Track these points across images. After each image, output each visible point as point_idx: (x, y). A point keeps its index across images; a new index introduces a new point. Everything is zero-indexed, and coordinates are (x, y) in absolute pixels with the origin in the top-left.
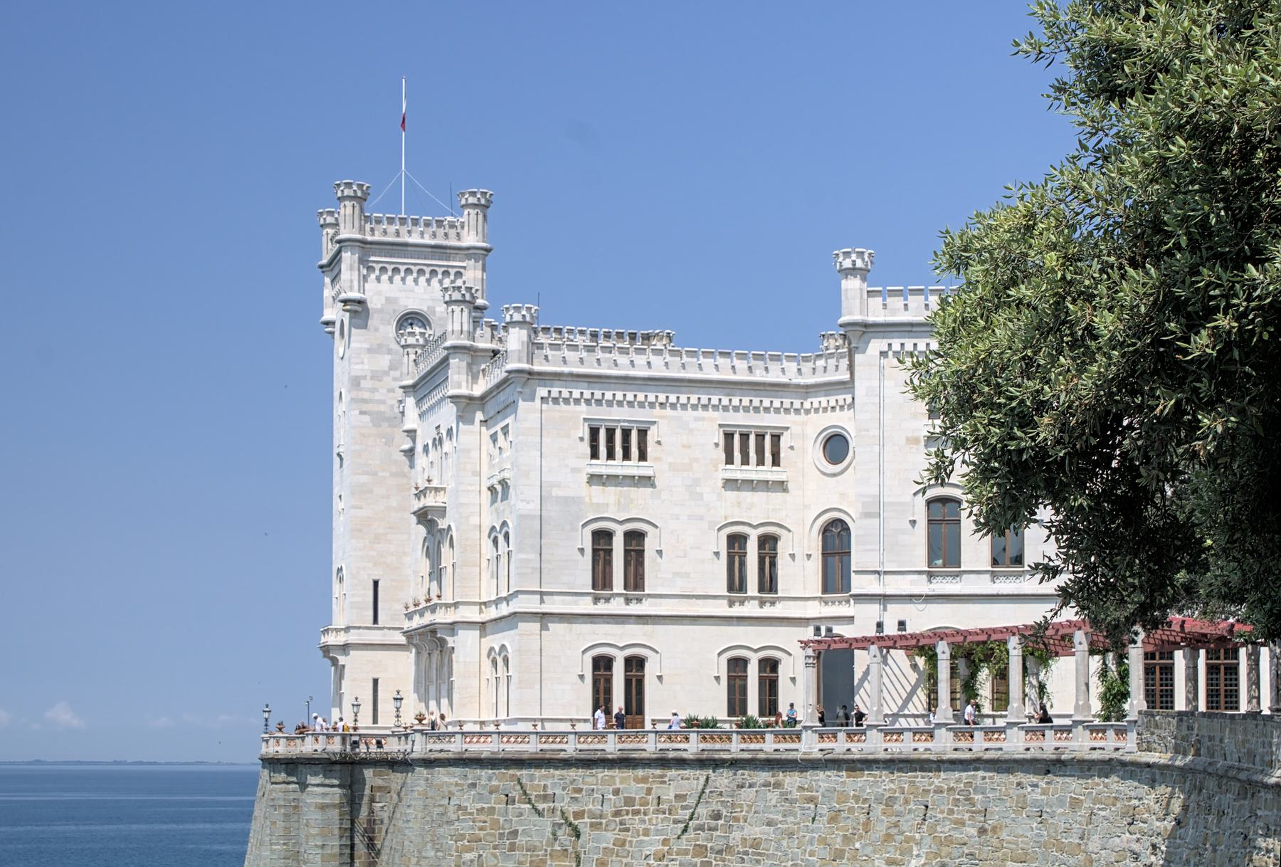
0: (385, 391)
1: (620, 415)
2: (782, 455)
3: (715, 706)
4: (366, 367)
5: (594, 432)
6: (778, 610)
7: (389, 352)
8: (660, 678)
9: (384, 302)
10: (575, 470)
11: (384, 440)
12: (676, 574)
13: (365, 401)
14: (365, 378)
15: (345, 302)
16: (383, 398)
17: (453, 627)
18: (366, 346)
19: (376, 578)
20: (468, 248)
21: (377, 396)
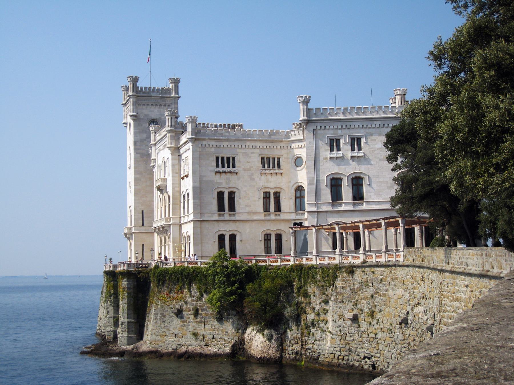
1: (226, 154)
2: (281, 164)
3: (260, 249)
4: (138, 138)
5: (217, 158)
6: (283, 217)
7: (146, 132)
8: (241, 241)
10: (211, 171)
12: (246, 206)
13: (138, 149)
15: (131, 116)
17: (169, 226)
18: (138, 131)
20: (172, 97)
21: (142, 148)
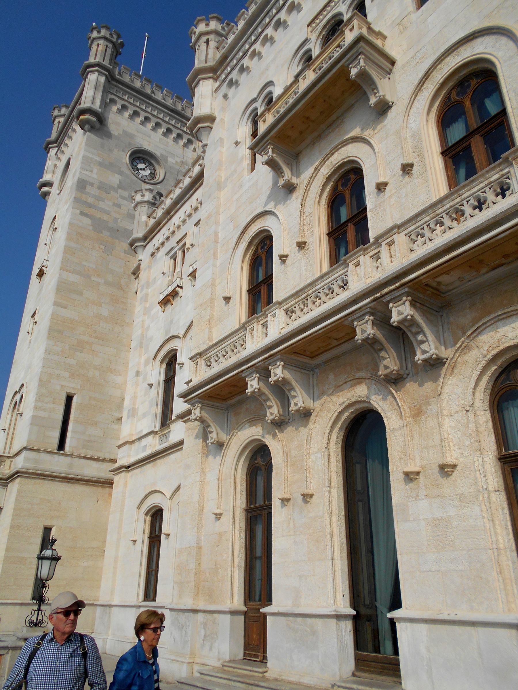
0: (111, 204)
4: (95, 176)
7: (121, 173)
9: (121, 133)
11: (103, 247)
13: (90, 206)
14: (92, 185)
16: (107, 209)
18: (97, 158)
19: (71, 391)
21: (102, 205)
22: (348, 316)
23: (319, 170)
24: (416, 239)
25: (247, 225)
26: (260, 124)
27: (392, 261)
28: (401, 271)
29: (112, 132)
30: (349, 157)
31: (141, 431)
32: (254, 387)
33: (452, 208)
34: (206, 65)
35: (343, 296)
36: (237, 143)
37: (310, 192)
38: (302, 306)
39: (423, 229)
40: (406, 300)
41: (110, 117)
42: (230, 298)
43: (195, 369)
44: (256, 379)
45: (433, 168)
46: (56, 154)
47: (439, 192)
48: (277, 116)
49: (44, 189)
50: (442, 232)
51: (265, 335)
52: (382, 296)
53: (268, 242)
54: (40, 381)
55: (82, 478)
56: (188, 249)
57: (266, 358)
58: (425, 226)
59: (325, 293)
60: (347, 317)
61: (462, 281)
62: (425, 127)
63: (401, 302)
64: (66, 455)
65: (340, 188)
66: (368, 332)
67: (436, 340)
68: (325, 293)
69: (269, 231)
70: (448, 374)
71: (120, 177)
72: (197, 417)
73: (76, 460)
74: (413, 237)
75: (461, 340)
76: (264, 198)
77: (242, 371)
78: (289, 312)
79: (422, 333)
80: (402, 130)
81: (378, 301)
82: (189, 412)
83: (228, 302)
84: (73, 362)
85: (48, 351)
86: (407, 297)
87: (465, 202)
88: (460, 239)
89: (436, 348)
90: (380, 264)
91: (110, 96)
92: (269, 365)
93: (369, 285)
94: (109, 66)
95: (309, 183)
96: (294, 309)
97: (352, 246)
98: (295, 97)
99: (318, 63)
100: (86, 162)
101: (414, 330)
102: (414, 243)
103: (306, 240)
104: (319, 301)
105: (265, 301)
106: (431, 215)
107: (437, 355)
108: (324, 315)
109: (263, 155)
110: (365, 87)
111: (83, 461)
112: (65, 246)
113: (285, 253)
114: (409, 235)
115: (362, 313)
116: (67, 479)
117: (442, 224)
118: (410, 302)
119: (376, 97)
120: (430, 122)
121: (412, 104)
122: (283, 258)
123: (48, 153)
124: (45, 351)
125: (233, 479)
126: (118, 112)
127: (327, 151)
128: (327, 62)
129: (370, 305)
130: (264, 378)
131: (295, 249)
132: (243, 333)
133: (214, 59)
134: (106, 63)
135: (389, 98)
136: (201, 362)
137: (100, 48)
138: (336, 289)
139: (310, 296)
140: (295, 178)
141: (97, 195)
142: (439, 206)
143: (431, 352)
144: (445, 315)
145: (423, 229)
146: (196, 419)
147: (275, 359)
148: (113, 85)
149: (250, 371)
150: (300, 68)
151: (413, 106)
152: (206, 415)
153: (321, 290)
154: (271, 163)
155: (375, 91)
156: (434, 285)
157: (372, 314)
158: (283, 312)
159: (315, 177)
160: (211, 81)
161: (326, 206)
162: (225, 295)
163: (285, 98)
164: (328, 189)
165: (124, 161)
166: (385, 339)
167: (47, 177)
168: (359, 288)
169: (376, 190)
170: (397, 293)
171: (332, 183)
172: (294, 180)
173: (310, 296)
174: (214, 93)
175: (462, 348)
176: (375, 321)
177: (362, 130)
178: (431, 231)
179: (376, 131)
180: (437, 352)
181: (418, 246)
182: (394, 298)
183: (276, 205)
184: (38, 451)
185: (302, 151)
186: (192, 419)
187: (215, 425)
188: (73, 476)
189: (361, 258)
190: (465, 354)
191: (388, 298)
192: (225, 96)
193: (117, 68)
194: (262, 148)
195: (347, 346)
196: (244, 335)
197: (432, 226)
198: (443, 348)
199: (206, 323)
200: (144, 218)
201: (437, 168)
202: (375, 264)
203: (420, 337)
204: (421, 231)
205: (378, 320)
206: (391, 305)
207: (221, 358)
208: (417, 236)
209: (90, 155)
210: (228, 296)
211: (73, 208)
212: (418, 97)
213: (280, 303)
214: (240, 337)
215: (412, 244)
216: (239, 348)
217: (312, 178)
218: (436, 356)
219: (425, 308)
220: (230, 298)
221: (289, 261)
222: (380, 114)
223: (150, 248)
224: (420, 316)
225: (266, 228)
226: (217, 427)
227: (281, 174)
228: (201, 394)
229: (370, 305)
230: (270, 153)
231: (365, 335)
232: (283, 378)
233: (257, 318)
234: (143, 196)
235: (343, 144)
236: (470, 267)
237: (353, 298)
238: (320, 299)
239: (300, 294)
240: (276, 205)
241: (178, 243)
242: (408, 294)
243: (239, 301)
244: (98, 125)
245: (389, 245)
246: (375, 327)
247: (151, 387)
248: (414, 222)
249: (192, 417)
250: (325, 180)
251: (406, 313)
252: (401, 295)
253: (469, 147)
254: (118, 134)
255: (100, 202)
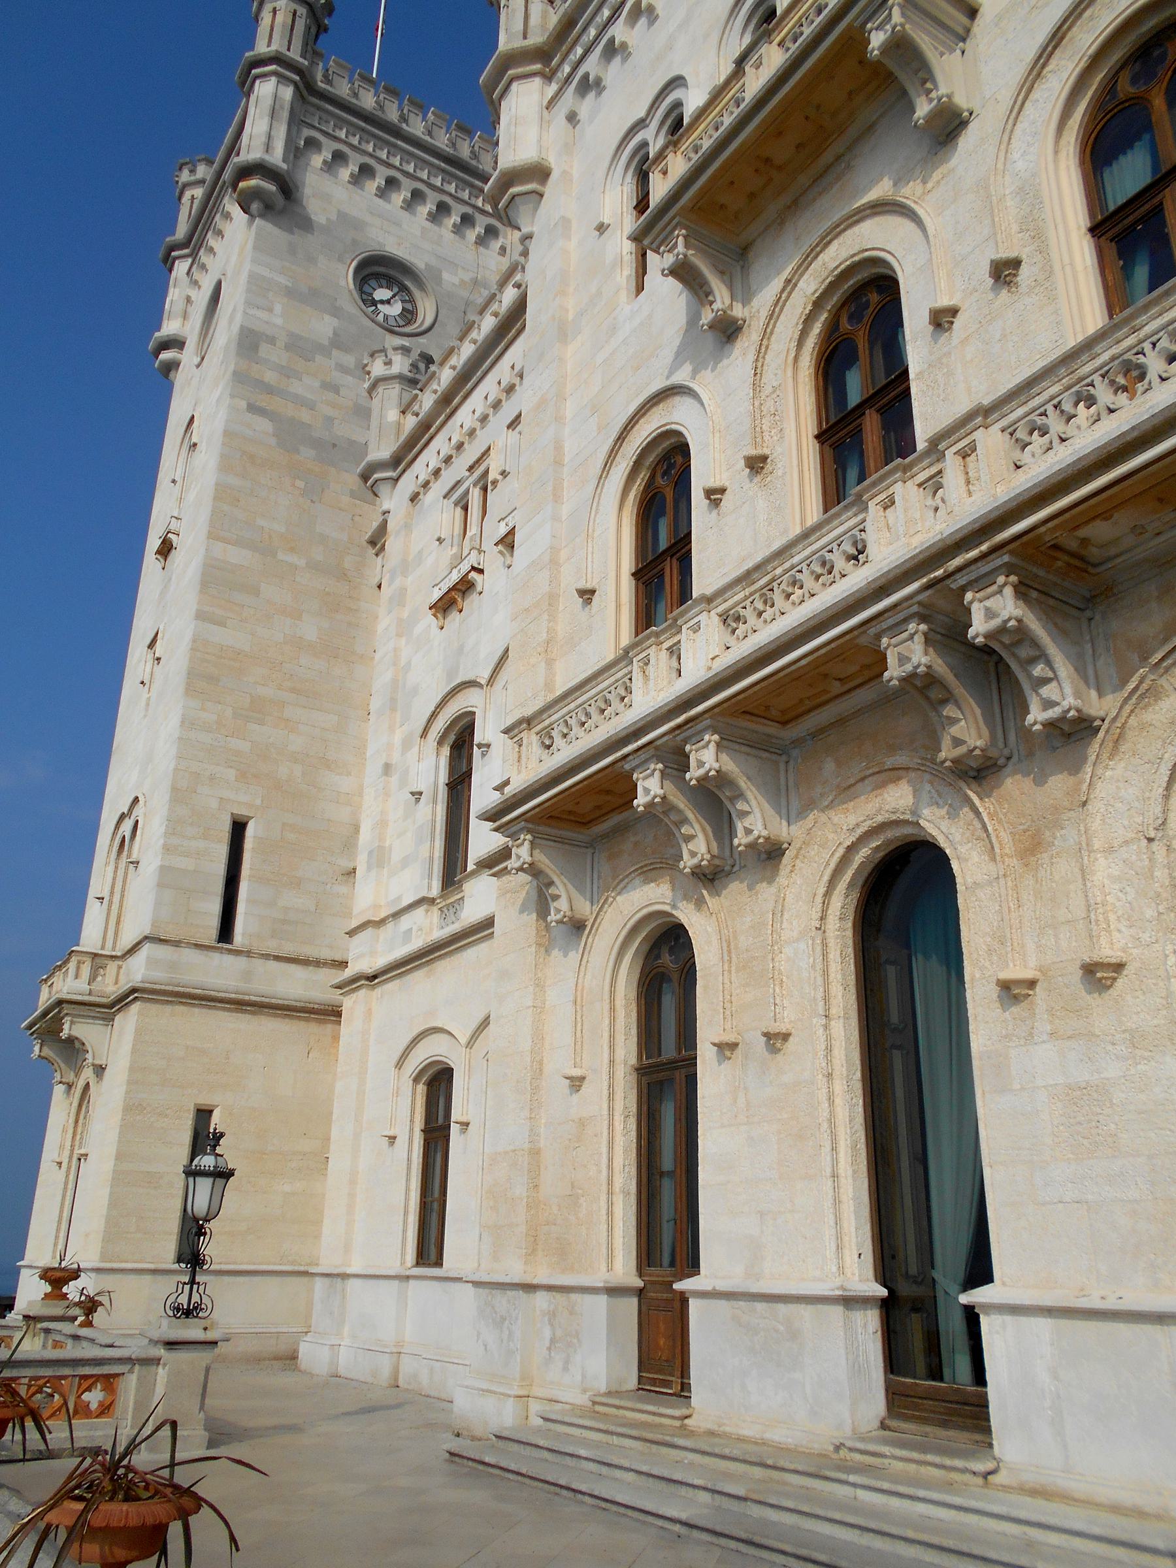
0: (317, 384)
4: (279, 321)
7: (336, 312)
9: (334, 217)
11: (300, 484)
13: (270, 390)
14: (272, 340)
18: (282, 280)
21: (296, 387)
22: (868, 625)
23: (795, 285)
24: (1027, 439)
25: (630, 422)
26: (655, 178)
27: (970, 494)
28: (993, 516)
29: (313, 217)
30: (867, 250)
31: (399, 898)
32: (652, 793)
33: (1116, 362)
34: (527, 43)
35: (857, 579)
36: (601, 228)
37: (773, 338)
38: (759, 605)
39: (1044, 414)
40: (1005, 584)
41: (307, 182)
42: (593, 592)
43: (516, 755)
44: (657, 774)
45: (1068, 269)
46: (188, 273)
47: (1084, 328)
48: (695, 157)
49: (165, 356)
50: (1091, 421)
51: (675, 674)
52: (949, 575)
53: (679, 460)
54: (174, 789)
55: (273, 1001)
56: (495, 483)
57: (679, 727)
58: (1049, 408)
59: (813, 572)
60: (864, 628)
61: (1141, 533)
62: (1051, 167)
63: (994, 588)
64: (238, 953)
65: (845, 325)
66: (915, 660)
67: (1075, 676)
68: (813, 572)
69: (679, 434)
70: (1105, 756)
71: (335, 322)
72: (524, 863)
73: (258, 962)
74: (1021, 434)
75: (1138, 675)
76: (667, 355)
77: (625, 757)
78: (731, 620)
79: (1042, 660)
80: (992, 178)
81: (938, 586)
82: (504, 854)
83: (588, 602)
84: (245, 746)
85: (187, 723)
86: (1007, 576)
87: (1147, 346)
88: (1135, 434)
89: (1077, 695)
90: (943, 500)
91: (307, 132)
92: (686, 741)
93: (918, 551)
94: (301, 60)
95: (772, 315)
96: (742, 612)
97: (875, 462)
98: (737, 112)
99: (790, 25)
100: (258, 287)
101: (1024, 652)
102: (1023, 448)
103: (766, 451)
104: (799, 592)
105: (675, 597)
106: (1064, 381)
107: (1078, 711)
108: (812, 623)
109: (664, 252)
110: (902, 76)
111: (273, 965)
112: (217, 484)
113: (717, 484)
114: (1010, 430)
115: (901, 616)
116: (240, 1005)
117: (1091, 401)
118: (1015, 587)
119: (931, 100)
120: (1063, 155)
121: (1019, 113)
122: (715, 495)
123: (170, 270)
124: (183, 722)
125: (608, 1001)
126: (325, 169)
127: (813, 239)
128: (813, 22)
129: (920, 597)
130: (675, 773)
131: (743, 473)
132: (625, 671)
133: (543, 27)
134: (295, 54)
135: (962, 101)
136: (531, 738)
137: (280, 18)
138: (840, 563)
139: (779, 581)
140: (740, 305)
141: (284, 364)
142: (1084, 358)
143: (1065, 704)
144: (1098, 617)
145: (1044, 414)
146: (521, 869)
147: (700, 727)
148: (314, 105)
149: (643, 756)
150: (747, 39)
151: (1020, 118)
152: (543, 860)
153: (804, 565)
154: (683, 272)
155: (929, 85)
156: (1073, 545)
157: (923, 618)
158: (716, 620)
159: (786, 301)
160: (537, 81)
161: (812, 370)
162: (582, 585)
163: (713, 114)
164: (817, 328)
165: (343, 283)
166: (956, 675)
167: (170, 327)
168: (893, 558)
169: (931, 328)
170: (983, 568)
171: (825, 315)
172: (738, 311)
173: (779, 581)
174: (545, 109)
175: (1139, 693)
176: (932, 635)
177: (895, 185)
178: (1065, 417)
179: (929, 185)
180: (1079, 703)
181: (1033, 456)
182: (976, 580)
183: (695, 373)
184: (177, 944)
185: (754, 240)
186: (512, 869)
187: (566, 881)
188: (253, 998)
189: (898, 488)
190: (1145, 707)
191: (961, 580)
192: (572, 118)
193: (321, 65)
194: (661, 237)
195: (865, 696)
196: (626, 675)
197: (1067, 406)
198: (1093, 694)
199: (539, 649)
200: (392, 415)
201: (1079, 267)
202: (930, 502)
203: (1038, 670)
204: (1039, 421)
205: (938, 633)
206: (969, 596)
207: (577, 730)
208: (1031, 433)
209: (266, 272)
210: (589, 586)
211: (232, 396)
212: (1034, 95)
213: (709, 600)
214: (617, 681)
215: (1018, 451)
216: (616, 704)
217: (779, 303)
218: (1076, 714)
219: (1051, 602)
220: (593, 592)
221: (727, 500)
222: (940, 144)
223: (408, 483)
224: (1039, 619)
225: (674, 427)
226: (570, 886)
227: (707, 296)
228: (532, 812)
229: (920, 597)
230: (680, 248)
231: (909, 668)
232: (717, 772)
233: (657, 635)
234: (388, 363)
235: (851, 221)
236: (1161, 500)
237: (879, 583)
238: (801, 587)
239: (756, 576)
240: (695, 373)
241: (471, 469)
242: (1009, 569)
243: (614, 599)
244: (280, 200)
245: (964, 455)
246: (931, 650)
247: (418, 800)
248: (1023, 398)
249: (512, 863)
250: (809, 307)
251: (1005, 615)
252: (995, 571)
253: (1159, 210)
254: (328, 219)
255: (292, 380)
